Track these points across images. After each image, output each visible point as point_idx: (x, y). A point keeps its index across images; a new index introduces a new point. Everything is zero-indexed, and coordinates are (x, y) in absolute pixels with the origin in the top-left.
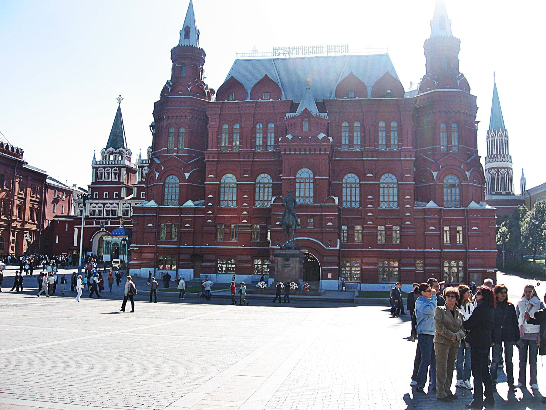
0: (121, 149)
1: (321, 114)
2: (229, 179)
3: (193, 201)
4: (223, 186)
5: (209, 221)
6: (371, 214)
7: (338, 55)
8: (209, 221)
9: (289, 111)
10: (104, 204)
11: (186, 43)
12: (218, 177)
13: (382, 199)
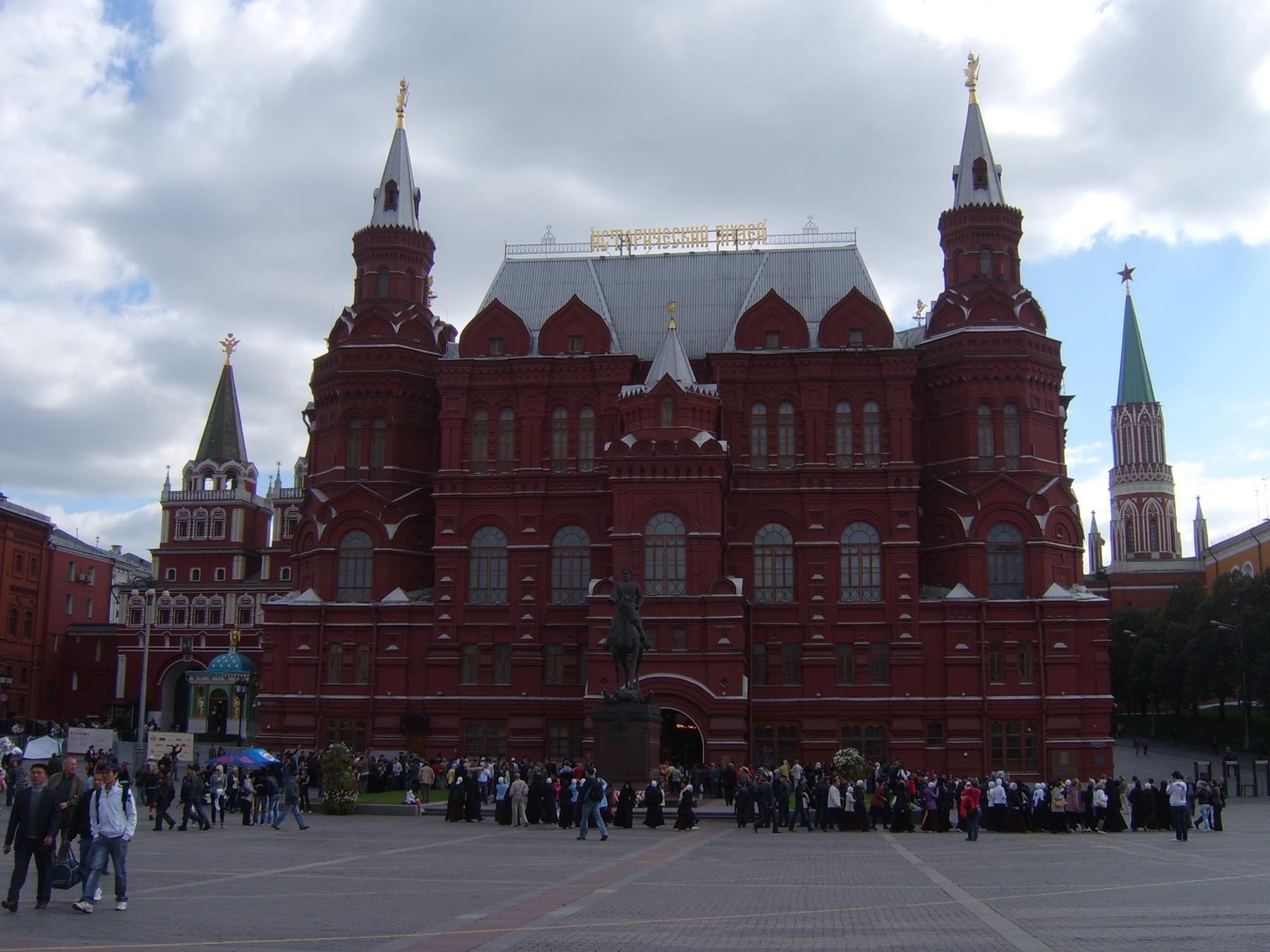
0: (232, 463)
1: (702, 388)
2: (490, 538)
5: (444, 636)
6: (821, 617)
8: (444, 636)
12: (465, 534)
13: (845, 581)
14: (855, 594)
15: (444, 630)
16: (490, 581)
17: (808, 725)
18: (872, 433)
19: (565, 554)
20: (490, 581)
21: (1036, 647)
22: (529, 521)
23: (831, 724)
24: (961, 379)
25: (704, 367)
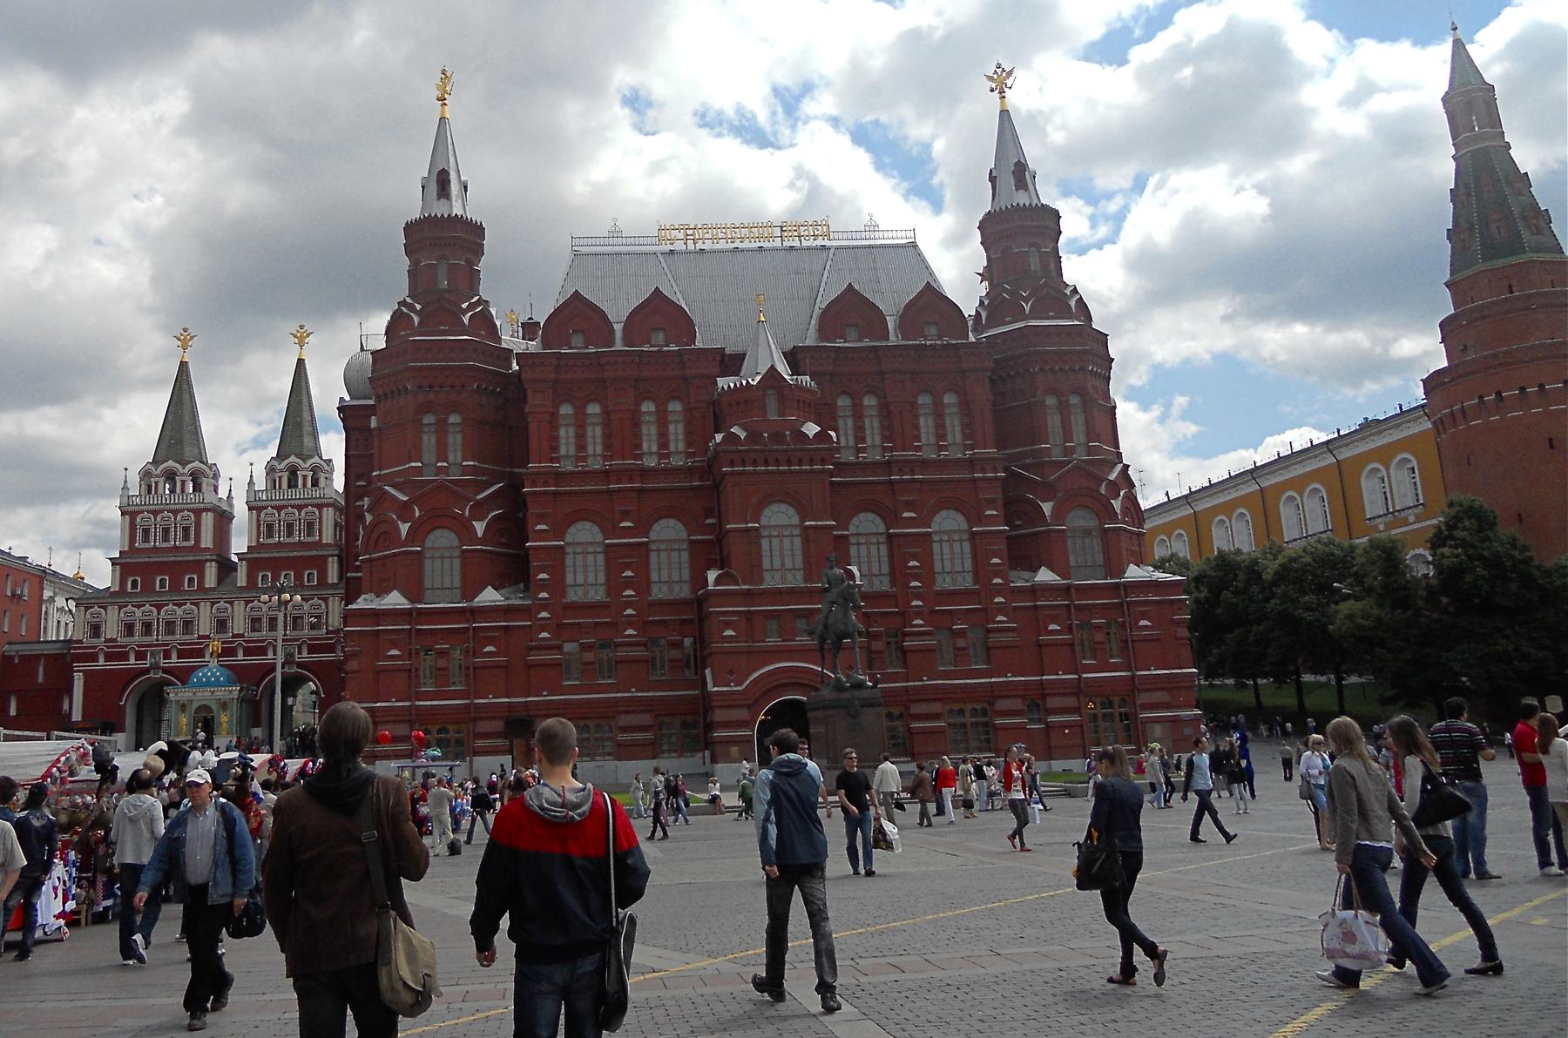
2: (584, 533)
5: (544, 635)
8: (544, 635)
9: (717, 370)
10: (159, 607)
11: (440, 209)
14: (948, 579)
16: (586, 577)
17: (916, 709)
18: (954, 425)
19: (663, 547)
20: (586, 577)
21: (1123, 625)
22: (625, 515)
23: (936, 708)
25: (792, 357)
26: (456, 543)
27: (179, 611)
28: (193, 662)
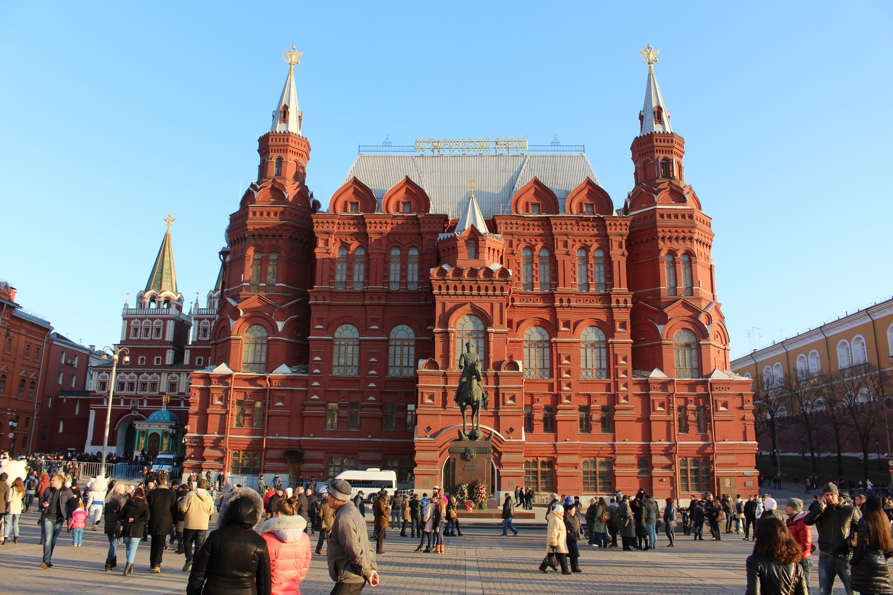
2: (347, 332)
3: (289, 366)
4: (337, 343)
5: (315, 397)
7: (511, 153)
8: (315, 397)
10: (139, 374)
12: (330, 328)
15: (316, 393)
19: (398, 343)
22: (374, 321)
24: (653, 239)
26: (265, 335)
27: (150, 377)
28: (152, 407)
